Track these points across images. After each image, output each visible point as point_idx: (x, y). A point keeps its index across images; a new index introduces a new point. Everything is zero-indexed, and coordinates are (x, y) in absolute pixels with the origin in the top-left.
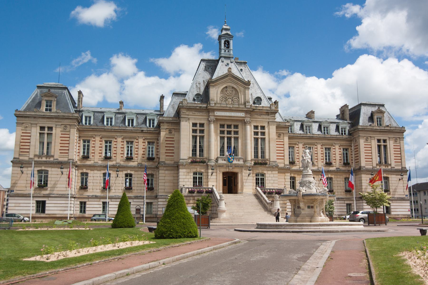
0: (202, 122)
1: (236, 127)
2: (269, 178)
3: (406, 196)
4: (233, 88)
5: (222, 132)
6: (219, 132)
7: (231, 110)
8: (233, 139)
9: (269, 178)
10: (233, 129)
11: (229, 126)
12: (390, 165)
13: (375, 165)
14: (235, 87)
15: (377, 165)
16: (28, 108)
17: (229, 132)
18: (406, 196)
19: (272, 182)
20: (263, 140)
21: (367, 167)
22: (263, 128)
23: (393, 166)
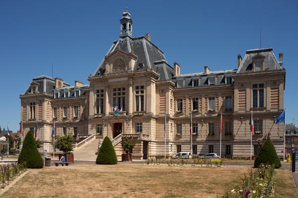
0: (102, 89)
1: (124, 89)
2: (145, 126)
3: (280, 137)
4: (121, 60)
5: (115, 94)
6: (112, 94)
7: (118, 77)
8: (258, 92)
9: (145, 126)
10: (121, 91)
11: (119, 89)
12: (266, 108)
13: (248, 109)
14: (122, 58)
15: (251, 109)
16: (26, 94)
17: (119, 94)
18: (280, 137)
19: (147, 128)
20: (142, 97)
21: (240, 112)
22: (142, 87)
23: (268, 109)
